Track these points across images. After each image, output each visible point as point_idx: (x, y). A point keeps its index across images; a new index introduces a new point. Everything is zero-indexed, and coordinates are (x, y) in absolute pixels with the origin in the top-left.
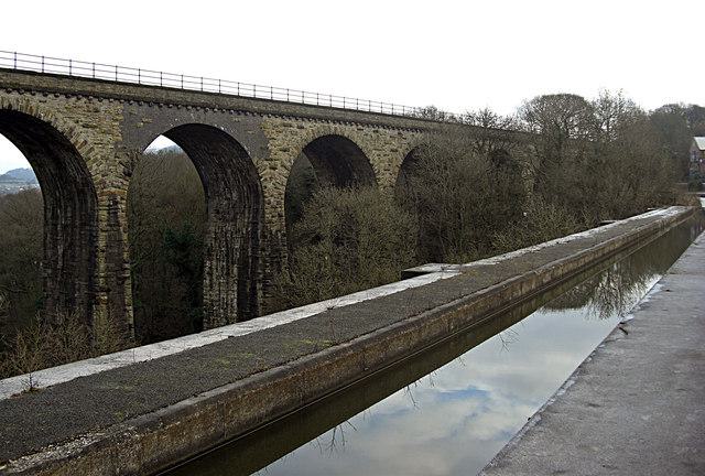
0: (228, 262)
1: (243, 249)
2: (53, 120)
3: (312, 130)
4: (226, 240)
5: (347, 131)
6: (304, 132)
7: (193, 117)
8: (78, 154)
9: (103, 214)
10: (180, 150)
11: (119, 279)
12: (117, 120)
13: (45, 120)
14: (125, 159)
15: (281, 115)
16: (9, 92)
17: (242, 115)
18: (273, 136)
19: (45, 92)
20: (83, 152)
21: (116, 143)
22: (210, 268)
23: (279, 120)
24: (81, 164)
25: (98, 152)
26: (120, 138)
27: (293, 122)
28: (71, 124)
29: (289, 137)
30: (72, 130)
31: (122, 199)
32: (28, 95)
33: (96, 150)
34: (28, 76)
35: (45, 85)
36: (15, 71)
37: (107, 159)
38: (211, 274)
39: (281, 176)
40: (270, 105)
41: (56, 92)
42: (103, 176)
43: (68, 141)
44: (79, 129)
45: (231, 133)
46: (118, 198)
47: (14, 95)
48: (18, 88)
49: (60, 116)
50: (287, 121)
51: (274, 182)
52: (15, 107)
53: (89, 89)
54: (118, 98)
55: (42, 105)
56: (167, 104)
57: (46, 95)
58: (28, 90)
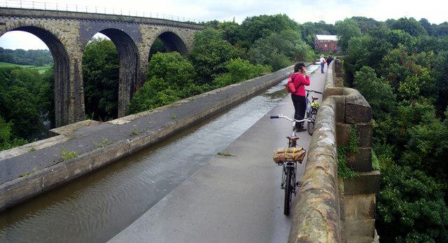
3: (160, 29)
5: (174, 30)
7: (110, 26)
14: (81, 44)
15: (148, 24)
19: (47, 18)
23: (147, 26)
24: (63, 47)
25: (70, 42)
27: (153, 27)
28: (58, 31)
30: (58, 33)
32: (39, 20)
39: (147, 49)
41: (50, 17)
44: (61, 33)
51: (144, 51)
54: (77, 19)
55: (45, 23)
58: (39, 17)
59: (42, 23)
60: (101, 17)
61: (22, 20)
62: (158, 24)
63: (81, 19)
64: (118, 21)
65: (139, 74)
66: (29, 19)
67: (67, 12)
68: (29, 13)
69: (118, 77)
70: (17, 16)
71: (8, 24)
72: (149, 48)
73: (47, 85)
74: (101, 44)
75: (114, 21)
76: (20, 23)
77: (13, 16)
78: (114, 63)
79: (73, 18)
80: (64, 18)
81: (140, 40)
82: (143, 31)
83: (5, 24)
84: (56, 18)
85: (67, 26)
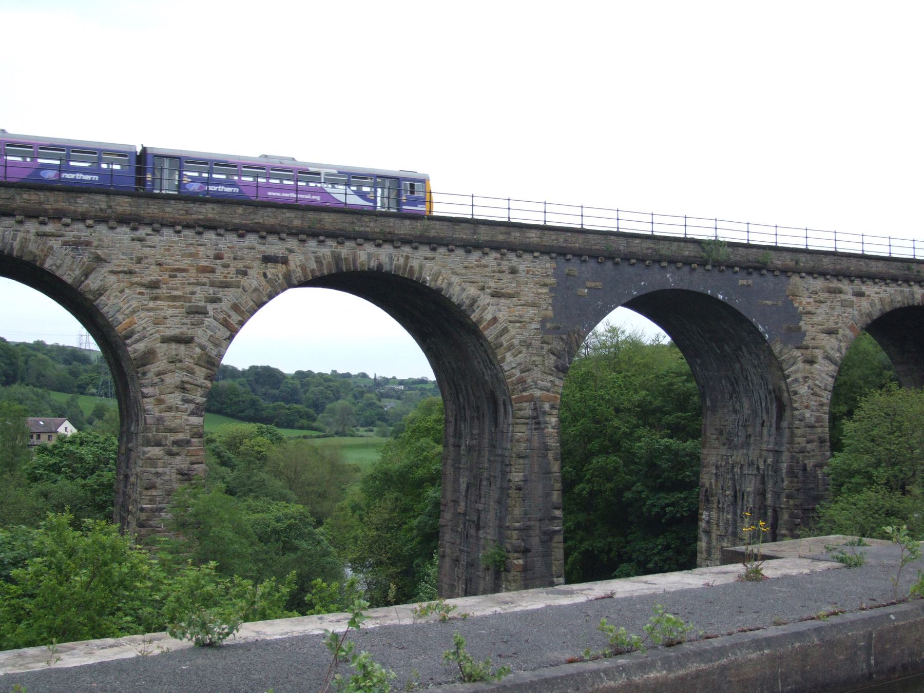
0: (735, 513)
2: (444, 286)
4: (733, 479)
6: (864, 303)
7: (671, 279)
8: (486, 340)
10: (666, 339)
11: (545, 533)
12: (545, 285)
13: (433, 285)
14: (558, 345)
15: (823, 274)
16: (379, 246)
17: (755, 275)
18: (809, 308)
19: (434, 243)
20: (490, 334)
21: (544, 321)
22: (708, 522)
23: (819, 284)
26: (550, 313)
27: (845, 286)
28: (472, 291)
29: (839, 309)
30: (474, 301)
31: (553, 407)
32: (407, 249)
33: (513, 332)
34: (407, 222)
35: (432, 233)
37: (529, 346)
38: (708, 533)
39: (824, 373)
40: (803, 258)
41: (449, 244)
42: (523, 371)
43: (468, 317)
44: (485, 299)
45: (737, 303)
46: (547, 406)
47: (387, 250)
48: (390, 239)
49: (455, 279)
50: (835, 284)
52: (386, 268)
53: (501, 238)
54: (546, 251)
55: (428, 264)
56: (626, 258)
57: (434, 249)
58: (406, 241)
59: (415, 263)
61: (346, 250)
62: (873, 278)
63: (561, 253)
64: (703, 264)
65: (791, 473)
66: (369, 248)
70: (333, 235)
71: (295, 261)
72: (832, 368)
75: (687, 262)
76: (337, 258)
77: (314, 235)
79: (529, 249)
80: (496, 247)
81: (795, 336)
82: (804, 302)
83: (285, 261)
84: (469, 247)
85: (507, 277)
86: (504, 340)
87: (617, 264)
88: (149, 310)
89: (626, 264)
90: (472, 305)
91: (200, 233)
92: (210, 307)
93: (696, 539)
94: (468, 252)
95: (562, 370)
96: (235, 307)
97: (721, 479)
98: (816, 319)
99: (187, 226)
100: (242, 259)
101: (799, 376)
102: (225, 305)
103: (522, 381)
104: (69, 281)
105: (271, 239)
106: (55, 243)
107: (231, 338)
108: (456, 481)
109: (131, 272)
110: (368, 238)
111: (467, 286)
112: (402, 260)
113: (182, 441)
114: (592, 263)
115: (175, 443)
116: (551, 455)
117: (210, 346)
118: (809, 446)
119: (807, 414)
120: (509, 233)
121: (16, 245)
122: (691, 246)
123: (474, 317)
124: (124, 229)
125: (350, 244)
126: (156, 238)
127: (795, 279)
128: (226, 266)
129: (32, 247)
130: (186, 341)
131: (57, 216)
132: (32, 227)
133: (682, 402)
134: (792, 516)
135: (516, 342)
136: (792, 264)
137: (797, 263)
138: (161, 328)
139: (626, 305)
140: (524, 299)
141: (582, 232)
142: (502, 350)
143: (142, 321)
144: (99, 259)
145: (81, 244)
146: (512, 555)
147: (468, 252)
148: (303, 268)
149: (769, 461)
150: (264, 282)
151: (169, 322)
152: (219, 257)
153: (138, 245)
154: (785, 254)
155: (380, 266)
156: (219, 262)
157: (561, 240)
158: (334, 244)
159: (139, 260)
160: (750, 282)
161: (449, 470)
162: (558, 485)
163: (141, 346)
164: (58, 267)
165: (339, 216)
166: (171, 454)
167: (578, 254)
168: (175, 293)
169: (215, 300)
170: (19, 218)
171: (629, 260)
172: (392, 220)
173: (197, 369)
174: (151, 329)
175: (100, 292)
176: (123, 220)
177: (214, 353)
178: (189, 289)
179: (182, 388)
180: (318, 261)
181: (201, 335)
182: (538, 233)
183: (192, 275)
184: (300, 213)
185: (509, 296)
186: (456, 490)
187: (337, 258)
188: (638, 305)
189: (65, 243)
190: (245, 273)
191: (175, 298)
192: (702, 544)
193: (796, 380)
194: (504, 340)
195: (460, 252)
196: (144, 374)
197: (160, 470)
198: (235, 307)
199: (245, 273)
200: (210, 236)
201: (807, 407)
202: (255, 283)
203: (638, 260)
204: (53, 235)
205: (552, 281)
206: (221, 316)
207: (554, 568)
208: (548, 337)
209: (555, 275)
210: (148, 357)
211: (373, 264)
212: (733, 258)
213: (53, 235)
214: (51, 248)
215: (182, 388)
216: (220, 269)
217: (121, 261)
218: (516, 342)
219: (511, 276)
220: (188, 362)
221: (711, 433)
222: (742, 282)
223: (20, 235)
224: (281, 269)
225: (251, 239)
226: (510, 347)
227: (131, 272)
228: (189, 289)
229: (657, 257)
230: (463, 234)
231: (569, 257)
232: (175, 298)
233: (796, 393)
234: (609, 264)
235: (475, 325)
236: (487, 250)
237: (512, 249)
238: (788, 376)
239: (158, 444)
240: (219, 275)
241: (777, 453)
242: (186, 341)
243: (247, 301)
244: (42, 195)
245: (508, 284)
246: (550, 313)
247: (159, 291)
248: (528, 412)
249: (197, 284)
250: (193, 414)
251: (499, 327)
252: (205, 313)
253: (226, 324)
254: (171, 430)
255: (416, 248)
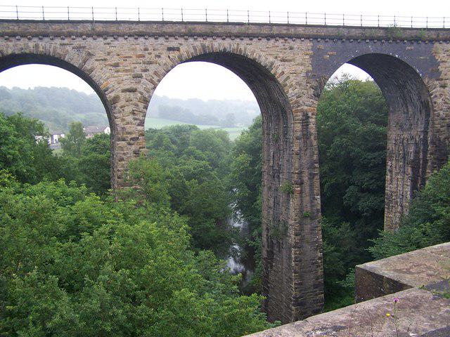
1: (417, 153)
2: (257, 57)
7: (371, 48)
9: (298, 127)
10: (372, 80)
14: (314, 84)
16: (224, 39)
17: (415, 44)
19: (251, 36)
20: (281, 80)
24: (281, 89)
26: (310, 68)
28: (271, 59)
30: (272, 64)
31: (313, 114)
32: (238, 40)
33: (292, 77)
34: (237, 27)
35: (250, 32)
36: (228, 24)
38: (391, 171)
44: (277, 63)
45: (405, 59)
46: (310, 114)
48: (230, 36)
52: (228, 50)
53: (284, 32)
54: (308, 37)
55: (249, 47)
56: (348, 39)
57: (251, 40)
59: (242, 47)
60: (353, 32)
61: (208, 42)
63: (315, 38)
64: (387, 40)
65: (432, 142)
66: (219, 41)
67: (288, 25)
68: (219, 30)
69: (384, 148)
70: (200, 35)
71: (183, 49)
73: (243, 157)
74: (348, 87)
75: (379, 39)
76: (203, 47)
77: (192, 35)
78: (379, 123)
79: (299, 37)
80: (282, 36)
82: (441, 56)
84: (269, 37)
86: (288, 83)
87: (343, 42)
88: (116, 77)
89: (348, 42)
90: (271, 66)
91: (136, 39)
92: (144, 74)
93: (385, 174)
94: (268, 40)
95: (317, 96)
96: (156, 73)
97: (397, 146)
98: (447, 65)
99: (130, 36)
100: (157, 50)
101: (438, 94)
102: (151, 72)
103: (297, 102)
104: (77, 66)
105: (171, 39)
106: (69, 48)
107: (155, 88)
108: (268, 151)
109: (105, 60)
110: (219, 36)
111: (268, 57)
112: (236, 46)
113: (134, 138)
114: (331, 42)
115: (131, 139)
116: (312, 137)
117: (145, 93)
118: (442, 129)
119: (441, 113)
120: (288, 29)
121: (52, 50)
122: (382, 31)
123: (273, 72)
124: (100, 39)
125: (209, 39)
126: (116, 42)
127: (437, 44)
128: (150, 54)
129: (59, 51)
130: (133, 91)
131: (69, 35)
132: (58, 41)
133: (379, 108)
134: (433, 163)
135: (294, 83)
136: (434, 37)
137: (438, 36)
138: (121, 85)
139: (349, 62)
140: (297, 62)
141: (325, 26)
142: (286, 88)
143: (112, 83)
144: (90, 54)
145: (81, 47)
146: (294, 186)
147: (268, 40)
148: (188, 52)
149: (422, 137)
150: (169, 61)
151: (125, 82)
152: (146, 49)
153: (108, 47)
154: (432, 32)
155: (225, 49)
156: (146, 52)
157: (315, 31)
158: (201, 39)
159: (109, 54)
160: (413, 48)
161: (265, 146)
162: (316, 152)
163: (113, 95)
164: (71, 60)
165: (204, 26)
166: (130, 144)
167: (323, 38)
168: (126, 68)
169: (146, 70)
170: (51, 37)
171: (349, 40)
172: (230, 26)
173: (139, 104)
174: (116, 86)
175: (92, 70)
176: (100, 35)
177: (147, 96)
178: (133, 66)
179: (133, 113)
180: (195, 48)
181: (140, 88)
182: (303, 28)
183: (134, 59)
184: (184, 25)
185: (290, 61)
186: (269, 155)
187: (203, 47)
188: (358, 62)
189: (73, 48)
190: (159, 57)
191: (127, 71)
192: (388, 177)
193: (436, 96)
194: (288, 83)
195: (264, 40)
196: (115, 107)
197: (125, 152)
198: (156, 73)
199: (159, 57)
200: (142, 39)
201: (441, 110)
202: (164, 61)
203: (354, 40)
204: (68, 44)
205: (311, 52)
206: (149, 78)
207: (315, 191)
208: (311, 80)
209: (312, 50)
210: (116, 99)
211: (222, 48)
212: (404, 36)
213: (68, 44)
214: (67, 51)
215: (133, 113)
216: (147, 56)
217: (100, 55)
218: (294, 83)
219: (289, 51)
220: (135, 101)
221: (392, 124)
222: (408, 48)
223: (53, 45)
224: (176, 54)
225: (161, 40)
226: (292, 85)
227: (105, 60)
228: (133, 66)
229: (363, 38)
230: (265, 31)
231: (319, 40)
232: (127, 71)
233: (435, 103)
234: (340, 42)
235: (274, 76)
236: (278, 38)
237: (290, 37)
238: (432, 95)
239: (124, 140)
240: (147, 58)
241: (425, 132)
242: (133, 91)
243: (161, 70)
244: (61, 26)
245: (289, 55)
246: (310, 68)
247: (119, 68)
248: (301, 117)
249: (137, 63)
250: (139, 125)
251: (285, 76)
252: (141, 77)
253: (152, 81)
254: (130, 133)
255: (242, 39)
